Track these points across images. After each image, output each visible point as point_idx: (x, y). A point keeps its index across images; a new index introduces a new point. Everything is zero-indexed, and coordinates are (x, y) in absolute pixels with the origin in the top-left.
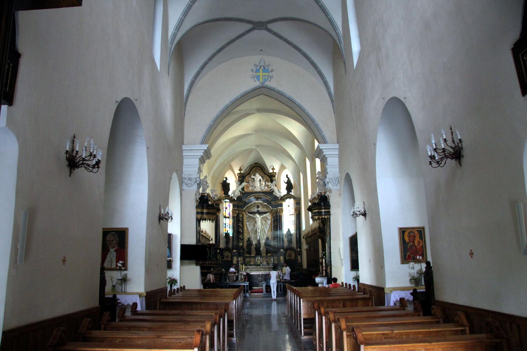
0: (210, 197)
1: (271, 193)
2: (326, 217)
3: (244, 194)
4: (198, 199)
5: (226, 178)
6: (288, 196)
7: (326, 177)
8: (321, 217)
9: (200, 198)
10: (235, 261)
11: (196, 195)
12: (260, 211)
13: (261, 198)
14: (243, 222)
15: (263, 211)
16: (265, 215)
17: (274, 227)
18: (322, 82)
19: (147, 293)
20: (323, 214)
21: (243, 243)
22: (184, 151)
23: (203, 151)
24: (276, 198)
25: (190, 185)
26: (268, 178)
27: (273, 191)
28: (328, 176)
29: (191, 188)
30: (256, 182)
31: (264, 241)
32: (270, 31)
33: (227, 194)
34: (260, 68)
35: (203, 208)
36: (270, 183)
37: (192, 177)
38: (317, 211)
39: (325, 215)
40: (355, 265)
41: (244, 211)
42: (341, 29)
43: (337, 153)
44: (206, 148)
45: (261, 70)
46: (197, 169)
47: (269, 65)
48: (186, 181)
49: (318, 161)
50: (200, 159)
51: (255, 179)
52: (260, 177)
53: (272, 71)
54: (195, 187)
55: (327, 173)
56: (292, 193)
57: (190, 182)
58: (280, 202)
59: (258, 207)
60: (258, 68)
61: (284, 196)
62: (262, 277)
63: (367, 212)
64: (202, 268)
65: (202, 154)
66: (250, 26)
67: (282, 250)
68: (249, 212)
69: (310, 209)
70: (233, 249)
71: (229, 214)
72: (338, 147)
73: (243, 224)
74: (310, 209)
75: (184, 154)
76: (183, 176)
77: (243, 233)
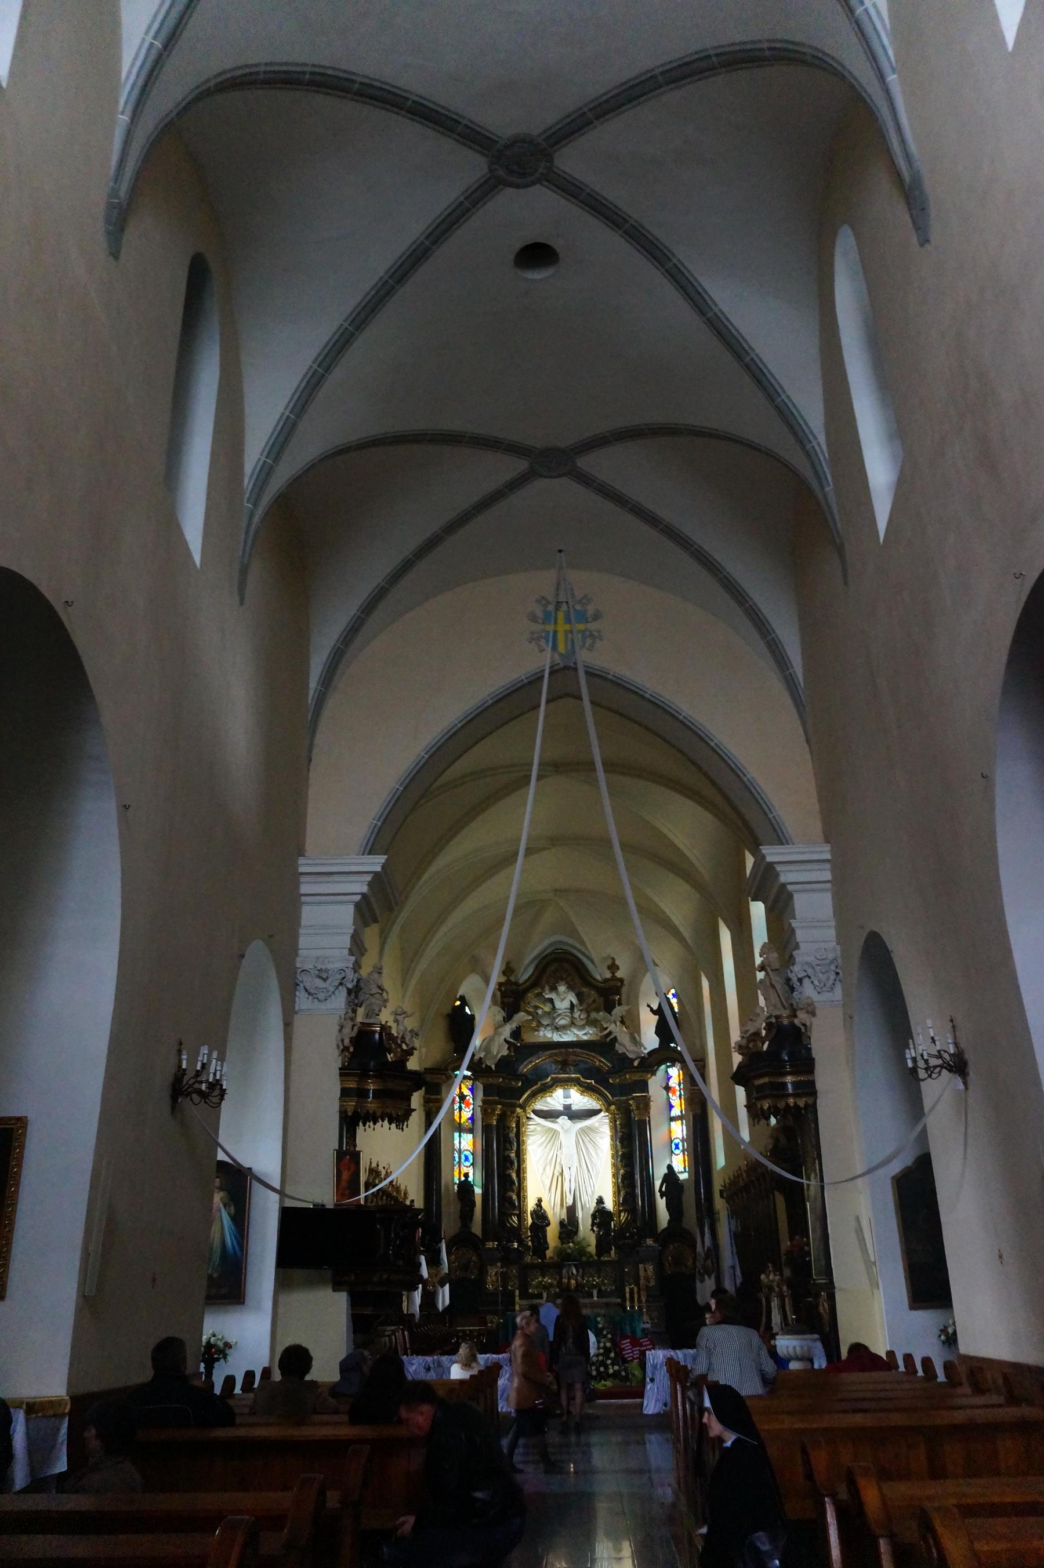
0: (390, 1034)
1: (605, 1046)
2: (801, 1103)
3: (521, 1048)
4: (347, 1042)
5: (462, 999)
6: (665, 1055)
7: (790, 960)
8: (781, 1105)
9: (354, 1041)
11: (342, 1027)
18: (762, 645)
19: (75, 1399)
20: (790, 1091)
21: (519, 1217)
22: (303, 879)
23: (369, 878)
24: (623, 1063)
25: (321, 996)
27: (615, 1039)
28: (800, 956)
29: (323, 1006)
32: (586, 480)
34: (557, 609)
35: (364, 1076)
37: (330, 966)
38: (766, 1080)
39: (795, 1095)
40: (928, 1283)
42: (822, 438)
43: (827, 875)
44: (378, 869)
45: (561, 615)
46: (347, 941)
47: (586, 600)
48: (309, 981)
49: (758, 910)
50: (358, 906)
52: (572, 997)
53: (597, 617)
54: (339, 1001)
55: (797, 947)
57: (320, 983)
60: (551, 608)
61: (652, 1052)
63: (969, 1056)
64: (355, 1301)
65: (365, 889)
66: (522, 465)
67: (649, 1242)
68: (535, 1112)
69: (740, 1077)
71: (472, 1118)
72: (828, 856)
74: (740, 1077)
75: (304, 889)
76: (298, 965)
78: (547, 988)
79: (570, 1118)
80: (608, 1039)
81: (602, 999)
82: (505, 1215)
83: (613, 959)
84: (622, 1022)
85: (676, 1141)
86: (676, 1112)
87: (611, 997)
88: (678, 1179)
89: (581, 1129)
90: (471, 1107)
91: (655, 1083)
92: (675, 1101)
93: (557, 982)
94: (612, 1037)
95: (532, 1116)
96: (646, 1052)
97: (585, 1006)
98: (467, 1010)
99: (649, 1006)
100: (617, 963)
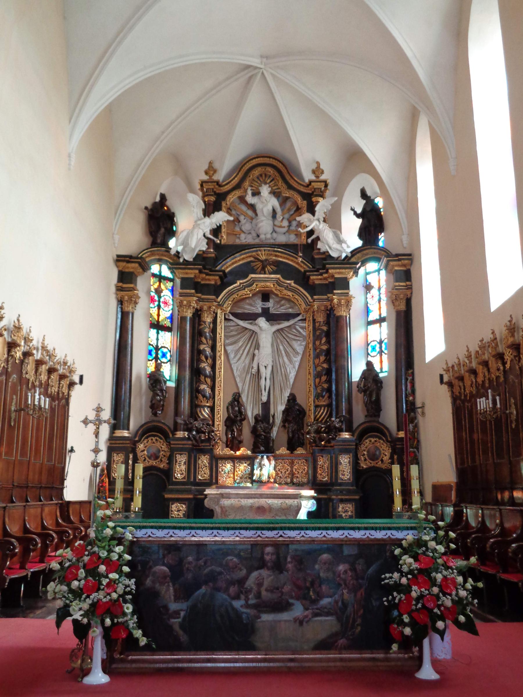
1: (309, 247)
5: (163, 197)
10: (180, 472)
12: (272, 311)
13: (277, 264)
14: (214, 340)
15: (282, 310)
16: (286, 324)
17: (317, 356)
21: (212, 409)
24: (325, 261)
26: (299, 199)
27: (318, 239)
30: (261, 217)
31: (281, 408)
33: (165, 244)
36: (305, 218)
41: (220, 306)
51: (259, 207)
52: (274, 202)
56: (382, 240)
58: (336, 273)
59: (266, 296)
61: (355, 252)
62: (278, 567)
67: (346, 435)
70: (176, 428)
71: (171, 318)
73: (213, 348)
77: (213, 378)
78: (250, 192)
79: (268, 320)
80: (310, 241)
81: (305, 202)
82: (194, 406)
83: (318, 163)
84: (325, 221)
85: (373, 344)
86: (374, 316)
87: (314, 199)
88: (377, 375)
89: (278, 330)
90: (171, 307)
91: (355, 284)
92: (373, 306)
93: (261, 186)
94: (314, 237)
95: (231, 317)
96: (349, 250)
97: (287, 216)
98: (174, 228)
99: (352, 209)
100: (321, 167)
